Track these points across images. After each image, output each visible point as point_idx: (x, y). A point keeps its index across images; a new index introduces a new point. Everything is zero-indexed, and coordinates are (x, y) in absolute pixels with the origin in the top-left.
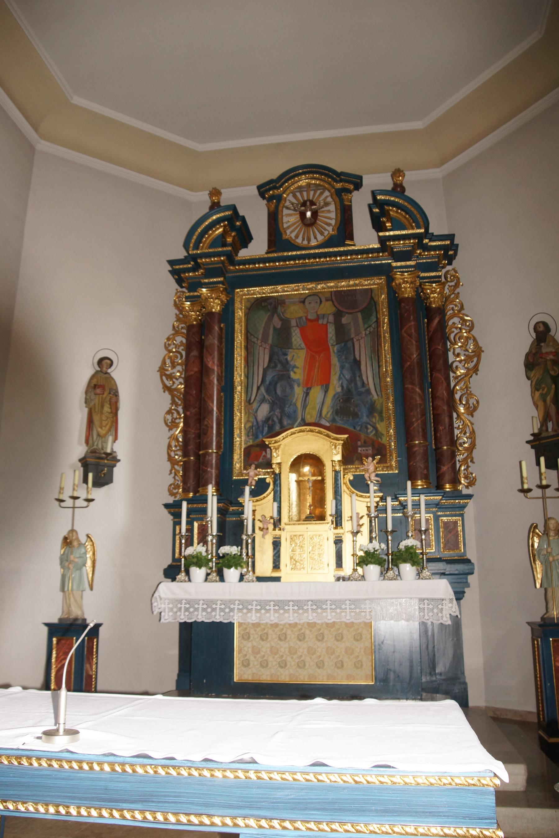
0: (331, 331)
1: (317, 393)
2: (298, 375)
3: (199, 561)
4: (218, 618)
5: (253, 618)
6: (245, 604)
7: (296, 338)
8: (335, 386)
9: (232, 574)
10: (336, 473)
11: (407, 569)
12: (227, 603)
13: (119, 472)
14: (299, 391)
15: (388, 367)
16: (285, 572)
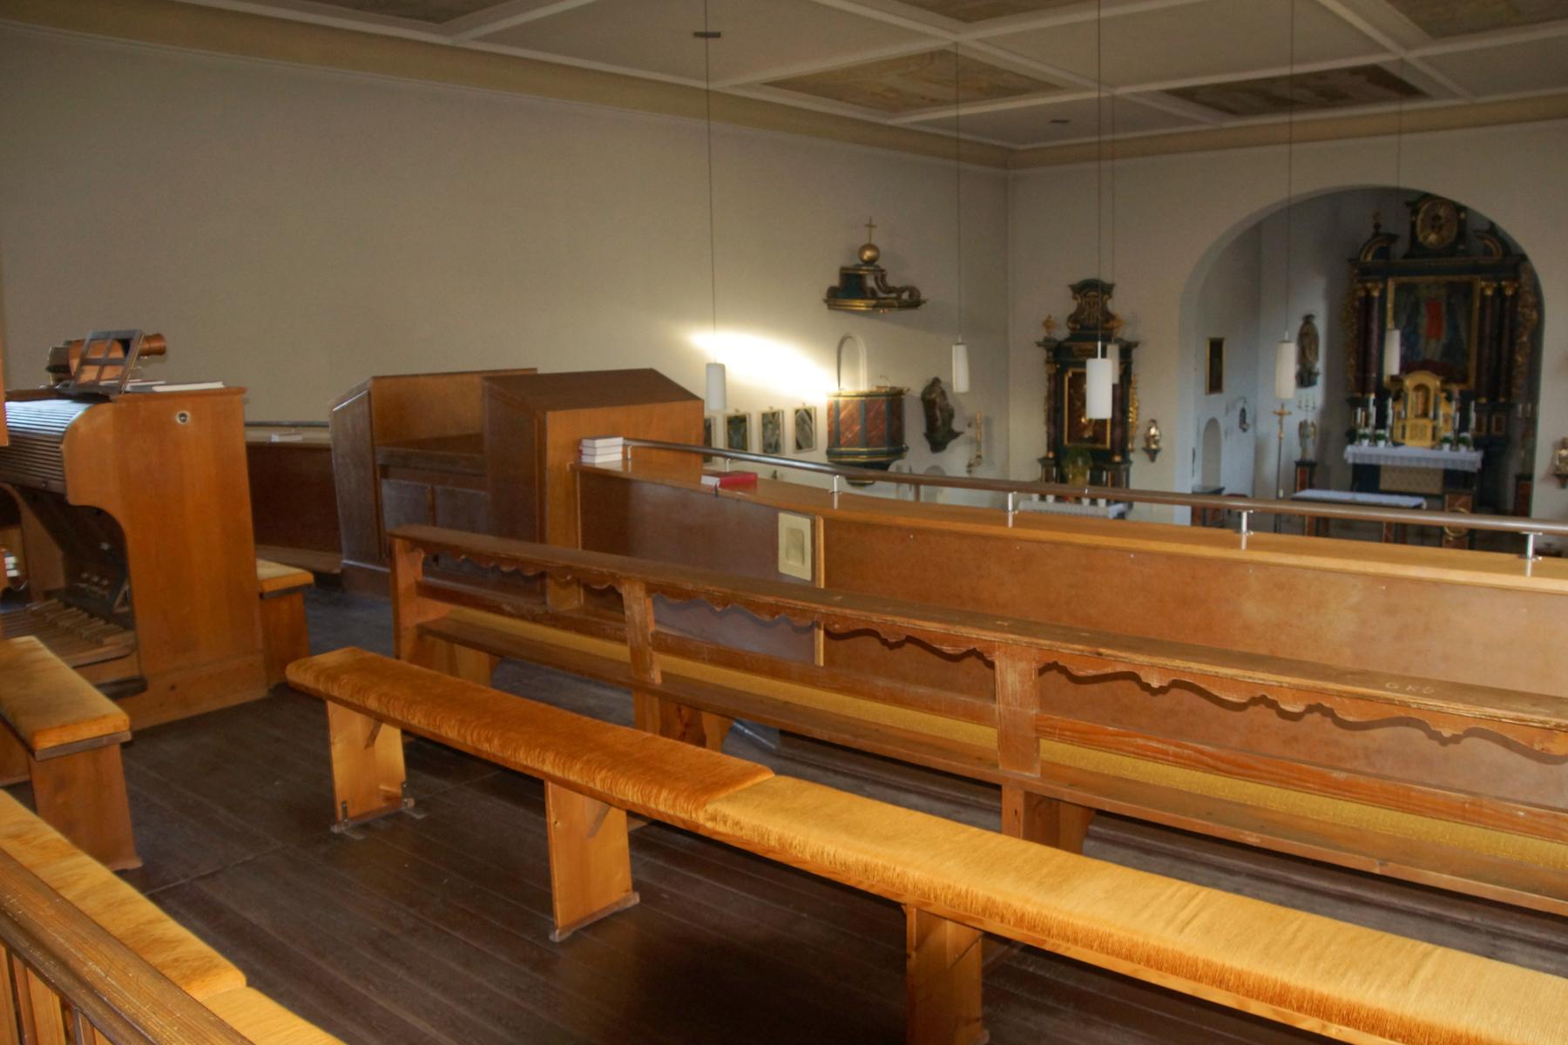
0: (1444, 309)
1: (1433, 343)
2: (1422, 331)
3: (1364, 436)
4: (1374, 462)
5: (1389, 463)
6: (1387, 457)
7: (1423, 310)
8: (1444, 340)
9: (1382, 444)
10: (1436, 395)
11: (1463, 449)
12: (1379, 456)
13: (1320, 380)
14: (1422, 341)
15: (1475, 333)
16: (1408, 442)
